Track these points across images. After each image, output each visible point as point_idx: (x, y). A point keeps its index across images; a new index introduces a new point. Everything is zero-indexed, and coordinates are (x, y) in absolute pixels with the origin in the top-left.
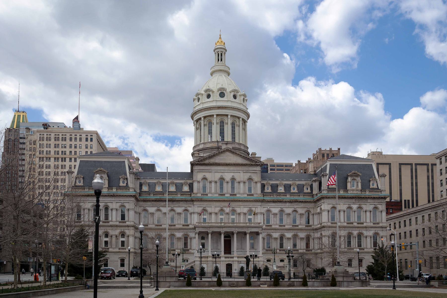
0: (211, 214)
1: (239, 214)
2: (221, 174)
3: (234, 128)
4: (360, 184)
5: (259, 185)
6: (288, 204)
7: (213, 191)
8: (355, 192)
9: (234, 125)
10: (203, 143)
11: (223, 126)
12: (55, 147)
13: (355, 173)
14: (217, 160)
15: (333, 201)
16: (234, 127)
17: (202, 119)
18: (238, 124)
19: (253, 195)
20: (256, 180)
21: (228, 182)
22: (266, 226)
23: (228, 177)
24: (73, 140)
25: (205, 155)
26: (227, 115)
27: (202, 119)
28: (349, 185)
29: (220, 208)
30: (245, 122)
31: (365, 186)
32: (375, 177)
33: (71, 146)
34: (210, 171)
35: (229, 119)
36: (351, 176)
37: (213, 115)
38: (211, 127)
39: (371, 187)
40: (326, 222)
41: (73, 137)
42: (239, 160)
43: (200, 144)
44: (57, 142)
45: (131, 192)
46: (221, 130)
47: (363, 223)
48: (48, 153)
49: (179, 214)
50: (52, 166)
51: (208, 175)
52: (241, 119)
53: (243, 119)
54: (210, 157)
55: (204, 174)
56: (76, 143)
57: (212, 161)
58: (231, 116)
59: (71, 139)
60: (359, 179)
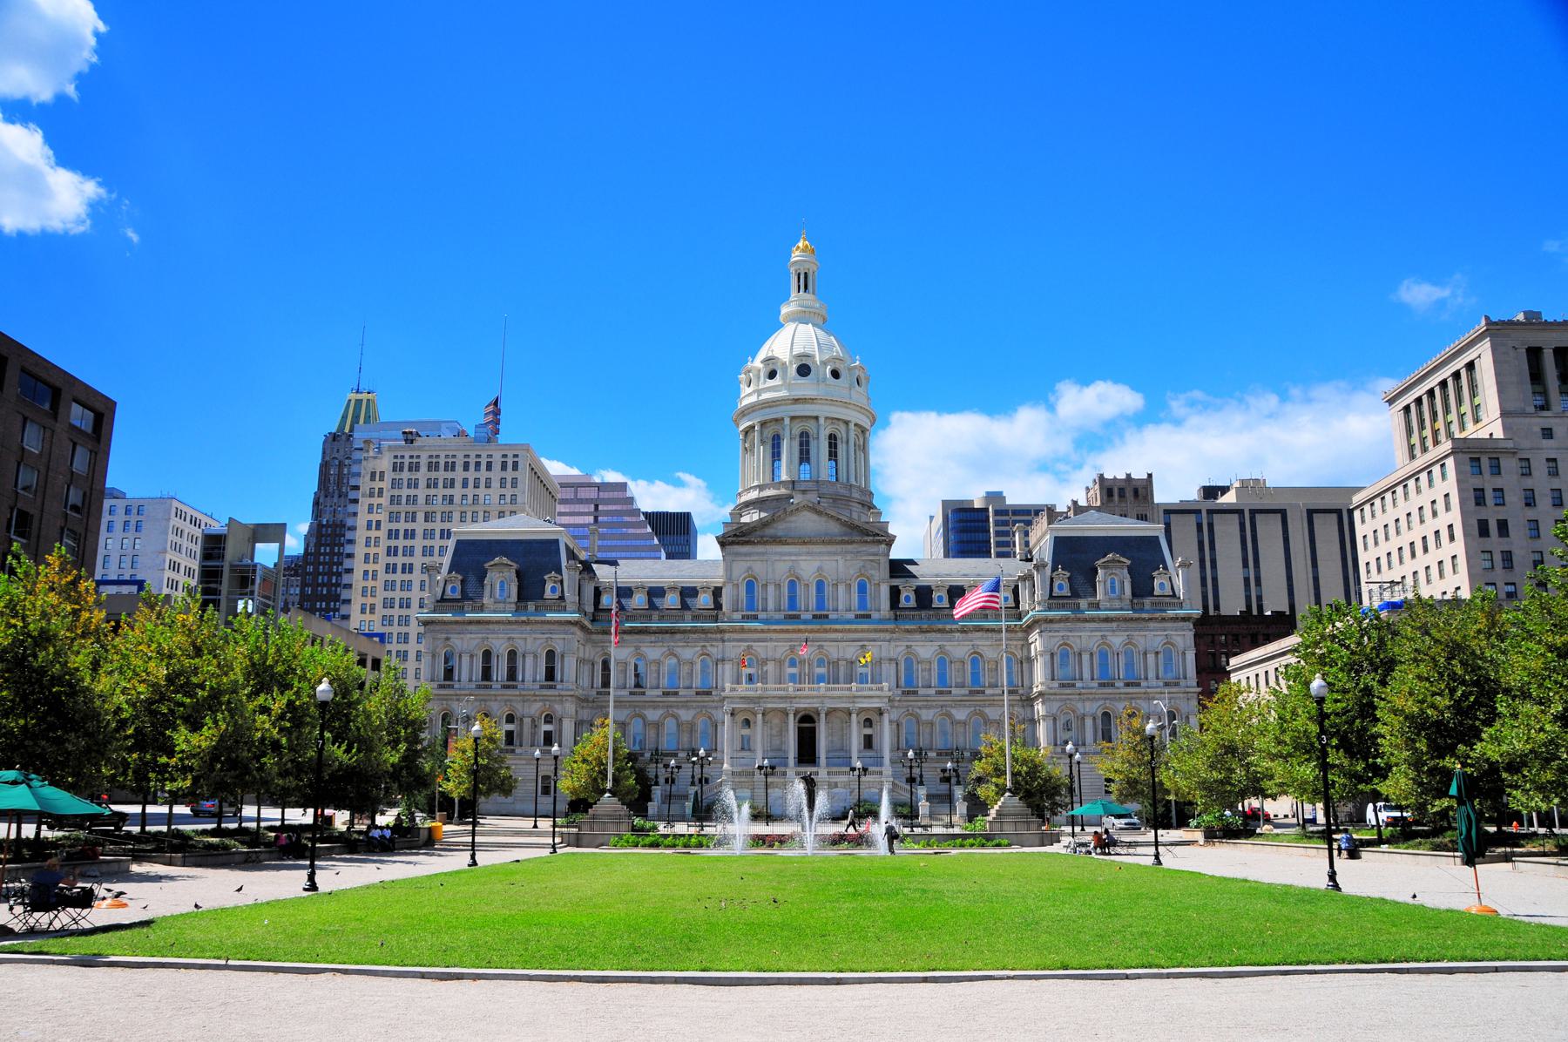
11: (808, 443)
12: (428, 486)
24: (472, 467)
25: (763, 515)
26: (817, 418)
33: (465, 484)
41: (472, 461)
42: (834, 528)
44: (433, 475)
48: (412, 500)
50: (419, 533)
54: (763, 524)
56: (477, 475)
57: (769, 531)
59: (466, 467)
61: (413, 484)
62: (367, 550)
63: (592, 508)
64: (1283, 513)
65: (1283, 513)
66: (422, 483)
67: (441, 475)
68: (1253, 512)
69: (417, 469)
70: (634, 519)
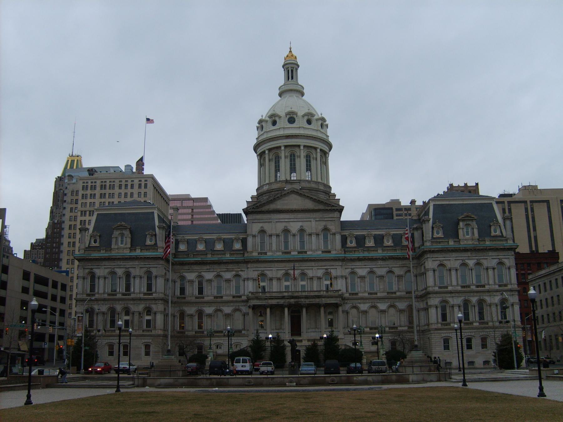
0: (271, 279)
1: (311, 279)
2: (284, 224)
3: (310, 162)
4: (476, 231)
5: (338, 238)
6: (380, 263)
7: (274, 248)
8: (470, 242)
9: (310, 157)
10: (268, 184)
13: (467, 216)
14: (279, 205)
15: (441, 257)
16: (310, 160)
17: (267, 152)
18: (315, 156)
19: (329, 252)
20: (333, 231)
21: (294, 235)
22: (350, 294)
23: (294, 227)
27: (267, 152)
28: (461, 232)
29: (284, 271)
30: (325, 154)
31: (484, 232)
32: (497, 221)
34: (270, 220)
35: (302, 151)
36: (463, 220)
37: (280, 147)
38: (279, 162)
39: (493, 234)
40: (432, 287)
42: (310, 205)
43: (264, 185)
45: (160, 253)
46: (291, 165)
47: (484, 286)
49: (228, 281)
51: (267, 227)
52: (319, 150)
53: (321, 150)
55: (261, 225)
57: (272, 207)
58: (304, 146)
60: (474, 224)
61: (93, 196)
62: (70, 231)
63: (190, 211)
64: (548, 202)
65: (548, 202)
66: (98, 196)
67: (108, 191)
68: (532, 202)
69: (95, 188)
70: (212, 216)
